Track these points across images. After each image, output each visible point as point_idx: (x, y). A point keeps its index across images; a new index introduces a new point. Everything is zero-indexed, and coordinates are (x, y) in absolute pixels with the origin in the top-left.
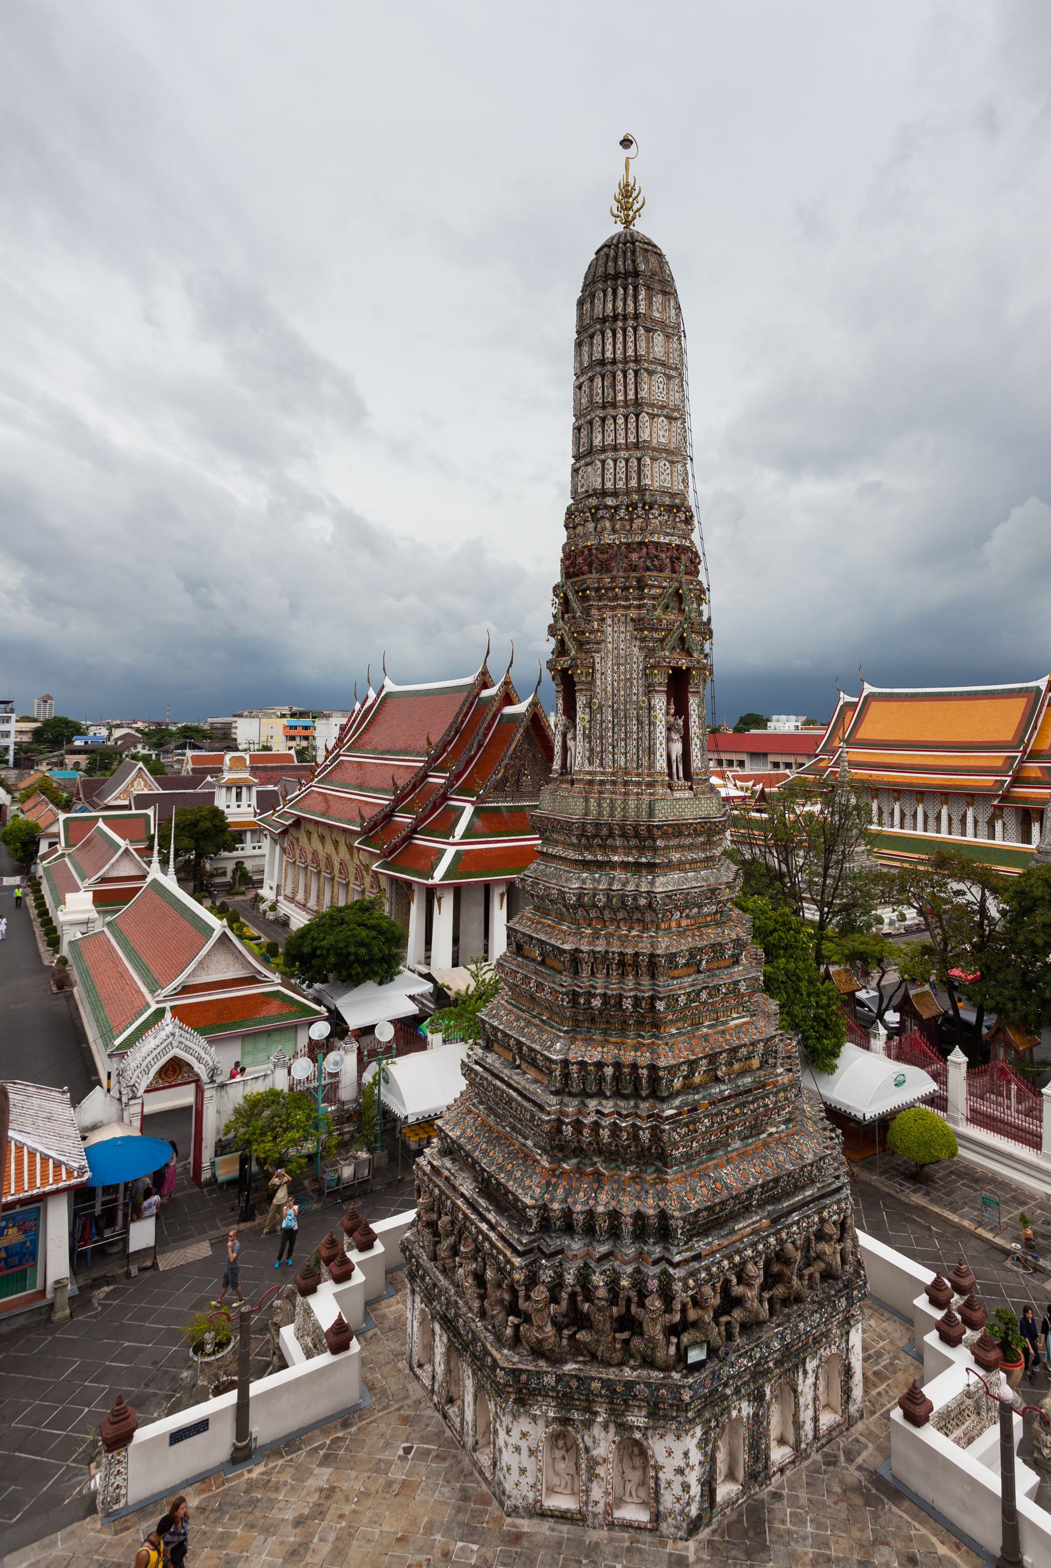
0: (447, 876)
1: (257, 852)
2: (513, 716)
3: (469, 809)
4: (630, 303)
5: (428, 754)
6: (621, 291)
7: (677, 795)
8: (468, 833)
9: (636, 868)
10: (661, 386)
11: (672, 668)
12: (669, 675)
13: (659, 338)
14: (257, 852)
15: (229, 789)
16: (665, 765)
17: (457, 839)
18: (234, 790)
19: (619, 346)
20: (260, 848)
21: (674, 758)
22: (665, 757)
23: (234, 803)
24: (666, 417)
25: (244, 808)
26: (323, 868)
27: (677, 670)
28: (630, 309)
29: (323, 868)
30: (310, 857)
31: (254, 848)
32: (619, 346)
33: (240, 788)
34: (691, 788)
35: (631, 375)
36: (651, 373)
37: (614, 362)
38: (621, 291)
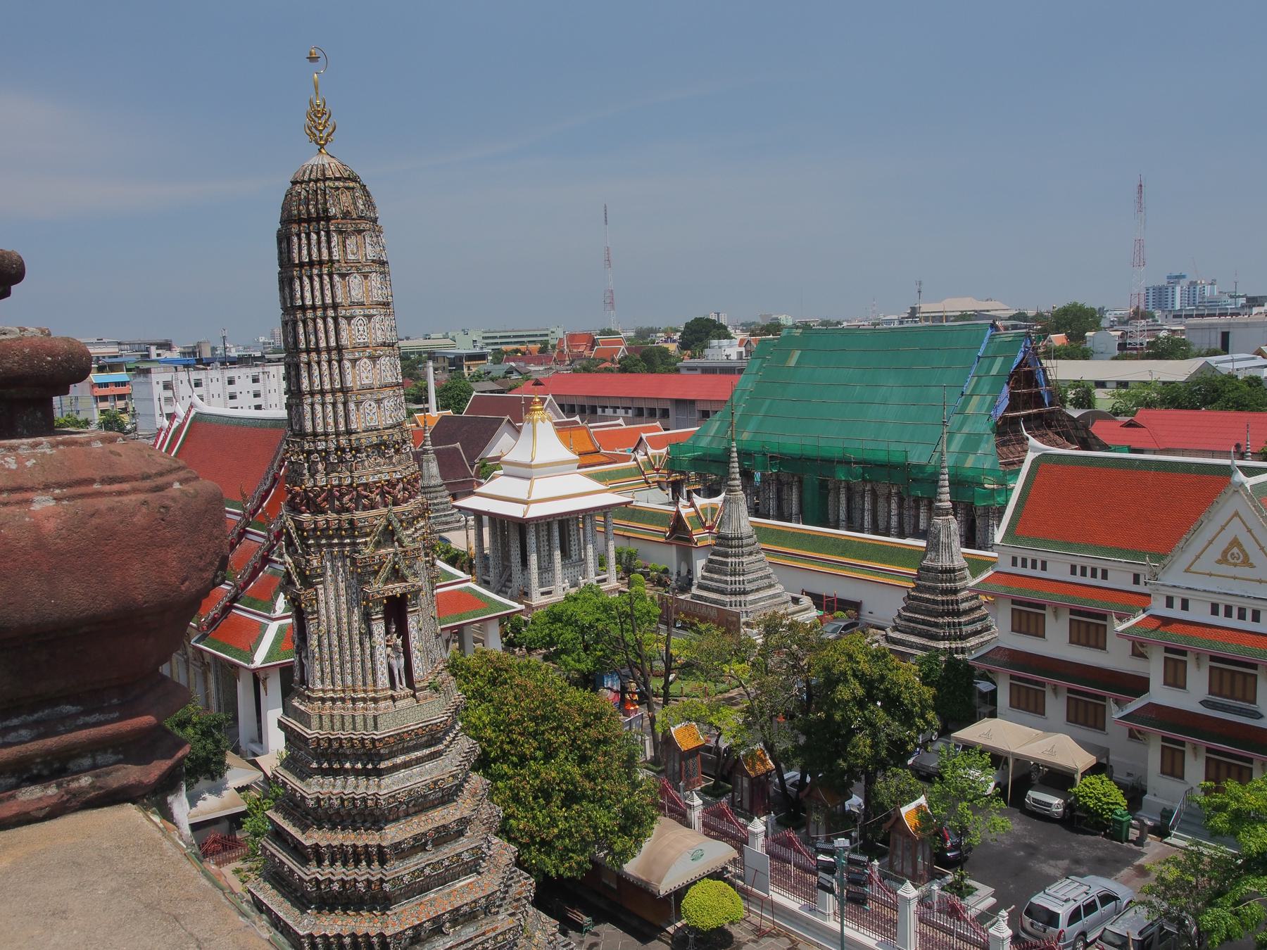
0: (269, 657)
4: (325, 251)
6: (314, 237)
7: (399, 704)
9: (367, 774)
10: (361, 328)
11: (387, 598)
12: (385, 606)
13: (355, 280)
16: (387, 681)
19: (318, 293)
21: (396, 672)
22: (386, 674)
24: (369, 358)
27: (391, 599)
28: (325, 257)
32: (318, 293)
34: (414, 696)
35: (330, 322)
36: (349, 319)
37: (314, 308)
38: (314, 237)
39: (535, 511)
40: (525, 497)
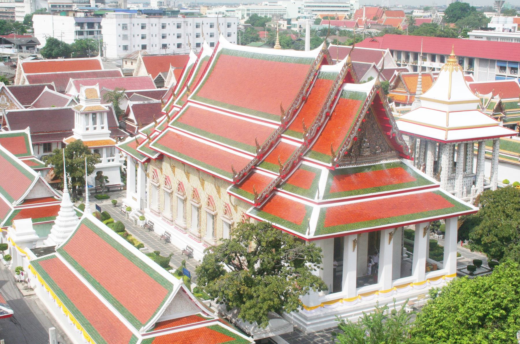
1: (111, 164)
2: (356, 95)
3: (325, 174)
5: (282, 120)
8: (329, 193)
14: (111, 164)
15: (87, 114)
17: (321, 200)
18: (91, 116)
20: (113, 160)
23: (91, 125)
25: (99, 131)
26: (189, 197)
29: (189, 197)
30: (175, 186)
31: (109, 161)
33: (94, 114)
39: (453, 136)
40: (444, 125)
